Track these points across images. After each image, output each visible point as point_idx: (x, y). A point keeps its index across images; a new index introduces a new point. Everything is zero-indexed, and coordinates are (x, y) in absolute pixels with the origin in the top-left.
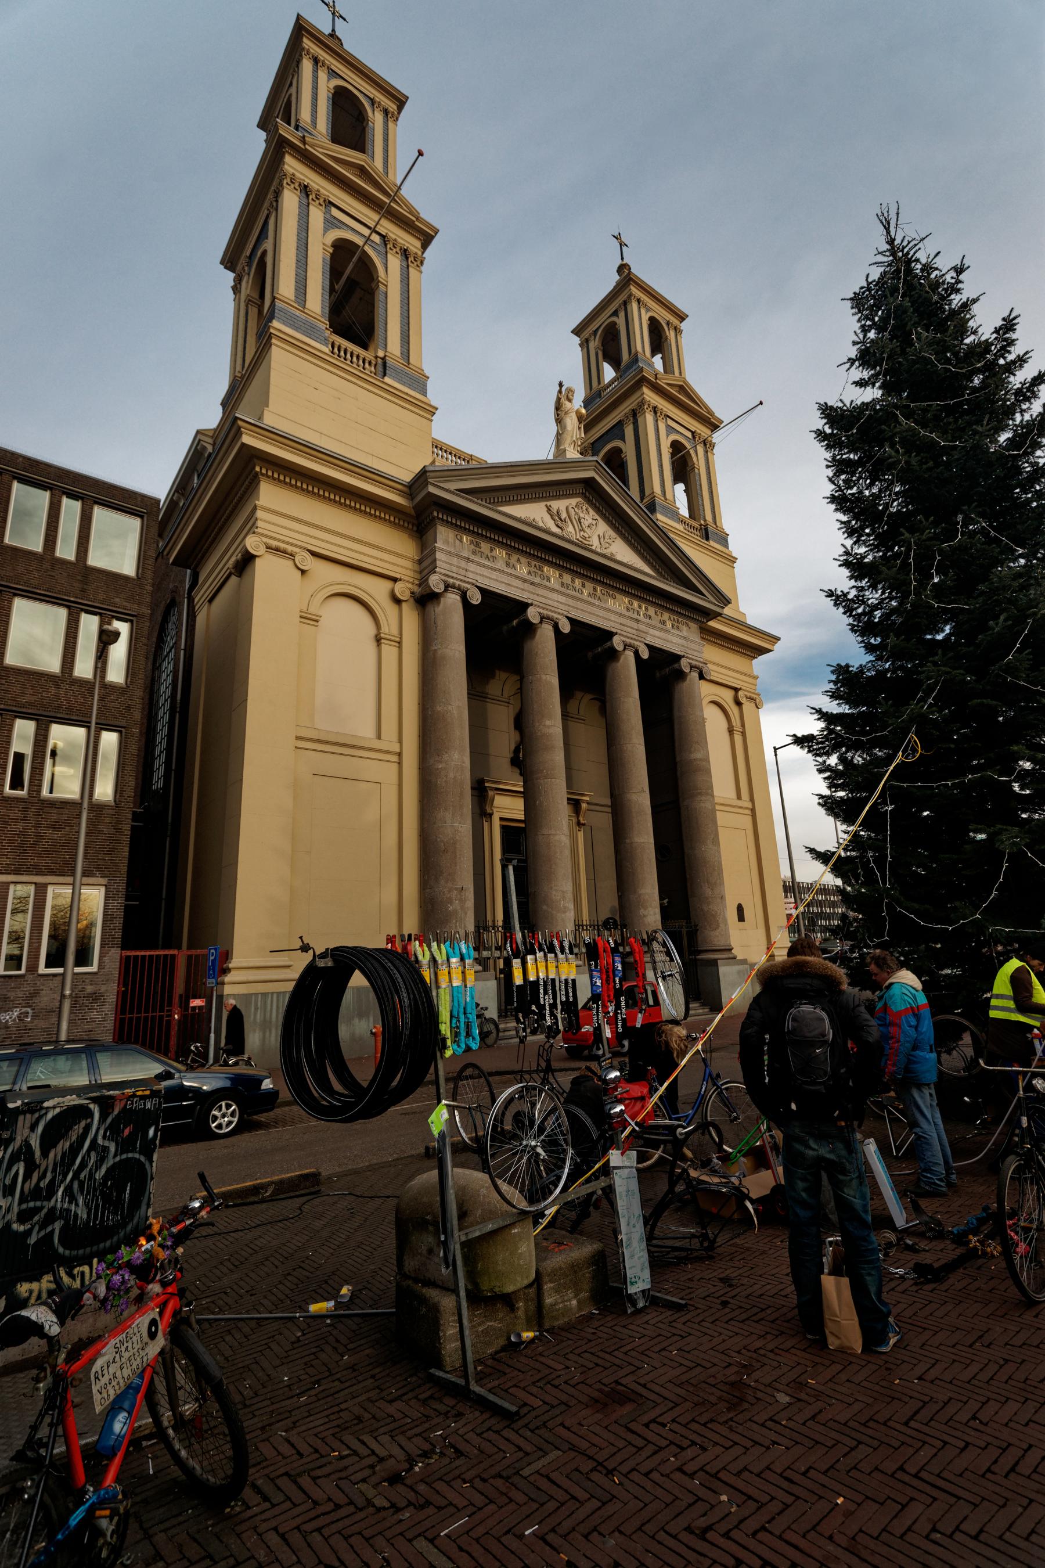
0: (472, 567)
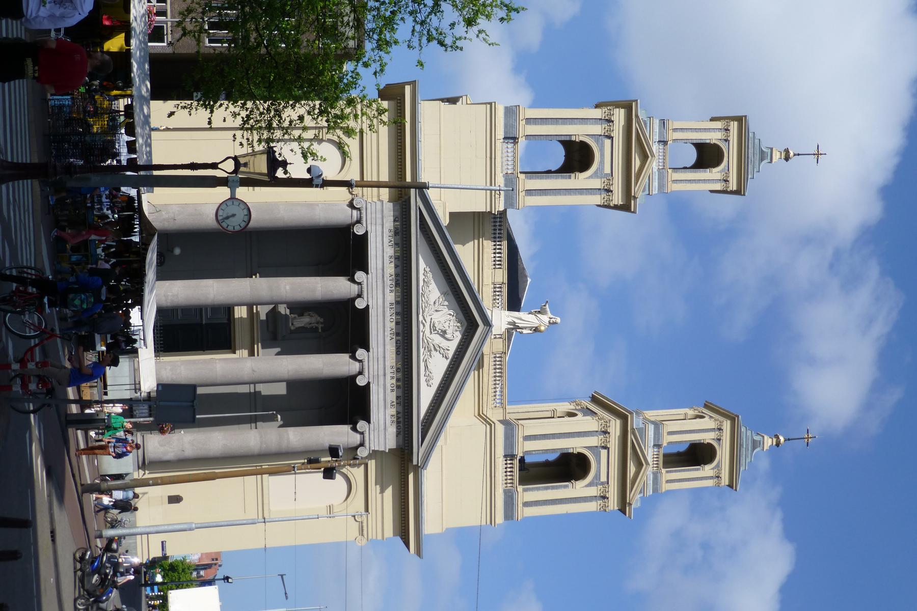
0: (379, 228)
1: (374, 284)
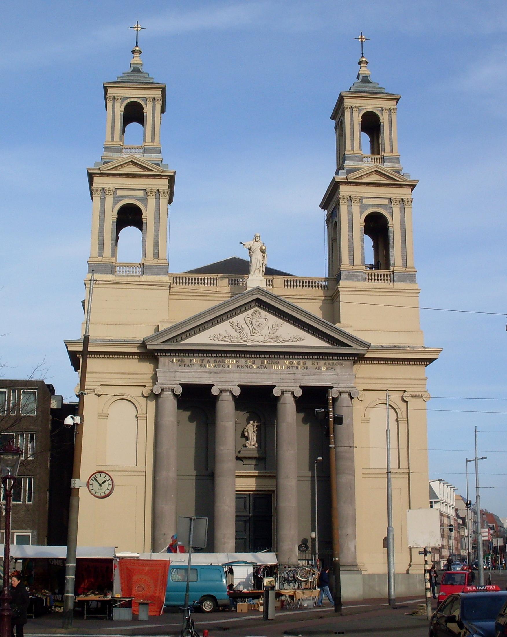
1: (224, 380)
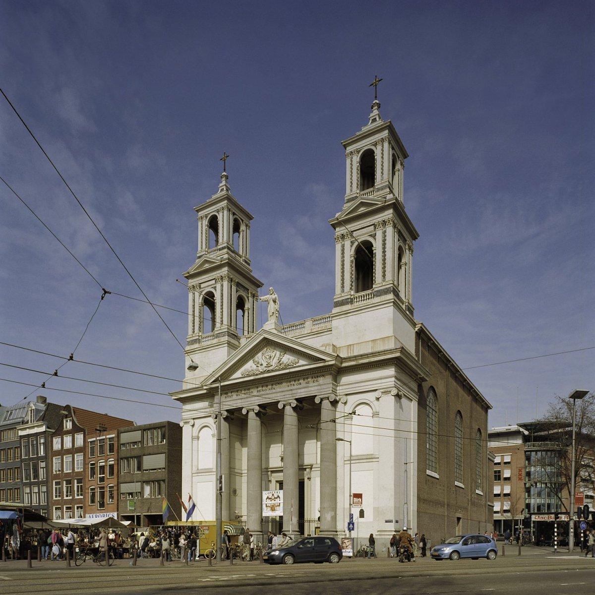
1: (250, 402)
